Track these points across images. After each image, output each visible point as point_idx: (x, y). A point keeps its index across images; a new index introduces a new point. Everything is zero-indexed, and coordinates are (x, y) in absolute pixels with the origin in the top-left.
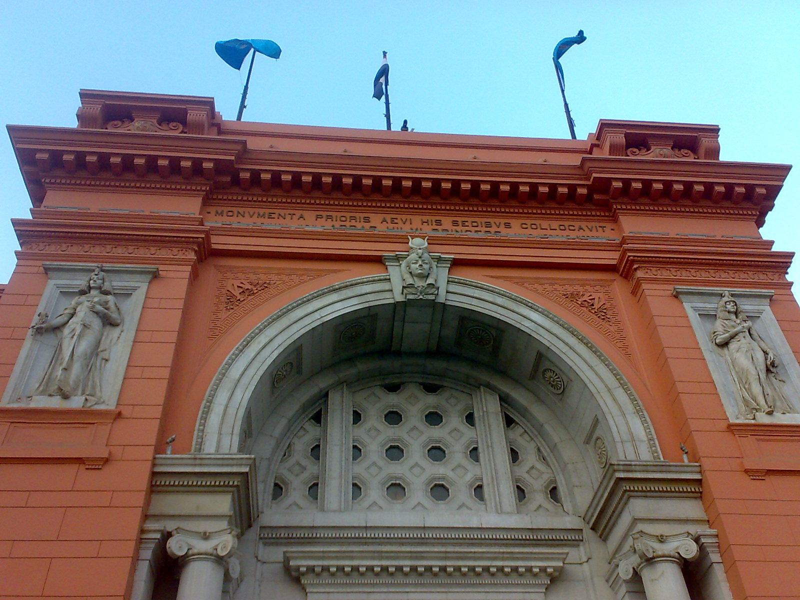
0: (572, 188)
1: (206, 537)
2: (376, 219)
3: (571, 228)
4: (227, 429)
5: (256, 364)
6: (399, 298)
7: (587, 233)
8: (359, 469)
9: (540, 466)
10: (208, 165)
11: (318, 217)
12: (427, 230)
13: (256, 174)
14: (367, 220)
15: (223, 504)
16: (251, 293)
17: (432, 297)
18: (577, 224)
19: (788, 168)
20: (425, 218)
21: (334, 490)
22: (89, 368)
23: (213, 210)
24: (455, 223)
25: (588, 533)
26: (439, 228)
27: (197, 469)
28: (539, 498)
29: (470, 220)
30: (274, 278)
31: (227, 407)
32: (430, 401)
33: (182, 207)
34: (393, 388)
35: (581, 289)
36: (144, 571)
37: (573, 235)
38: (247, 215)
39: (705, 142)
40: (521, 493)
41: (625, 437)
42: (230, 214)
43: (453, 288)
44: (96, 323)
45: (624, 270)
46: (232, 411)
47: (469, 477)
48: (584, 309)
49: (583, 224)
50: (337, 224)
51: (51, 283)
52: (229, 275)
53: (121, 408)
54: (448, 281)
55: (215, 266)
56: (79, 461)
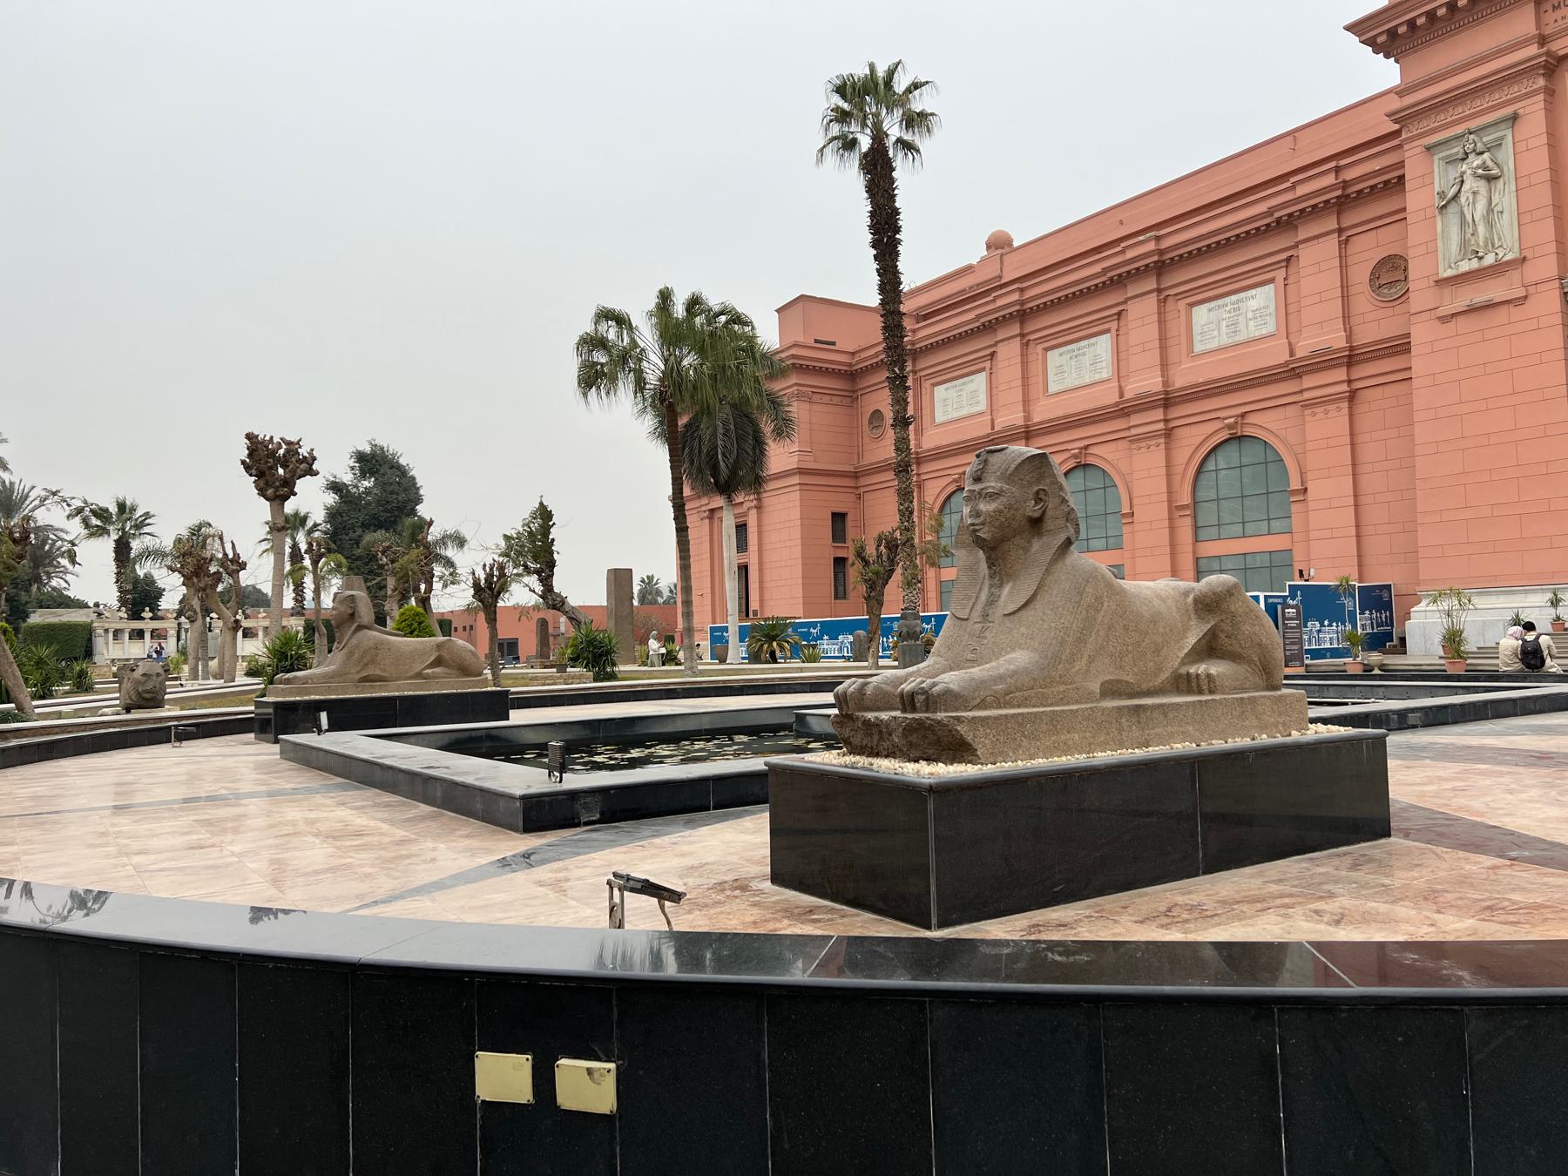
22: (1490, 225)
44: (1482, 186)
51: (1436, 157)
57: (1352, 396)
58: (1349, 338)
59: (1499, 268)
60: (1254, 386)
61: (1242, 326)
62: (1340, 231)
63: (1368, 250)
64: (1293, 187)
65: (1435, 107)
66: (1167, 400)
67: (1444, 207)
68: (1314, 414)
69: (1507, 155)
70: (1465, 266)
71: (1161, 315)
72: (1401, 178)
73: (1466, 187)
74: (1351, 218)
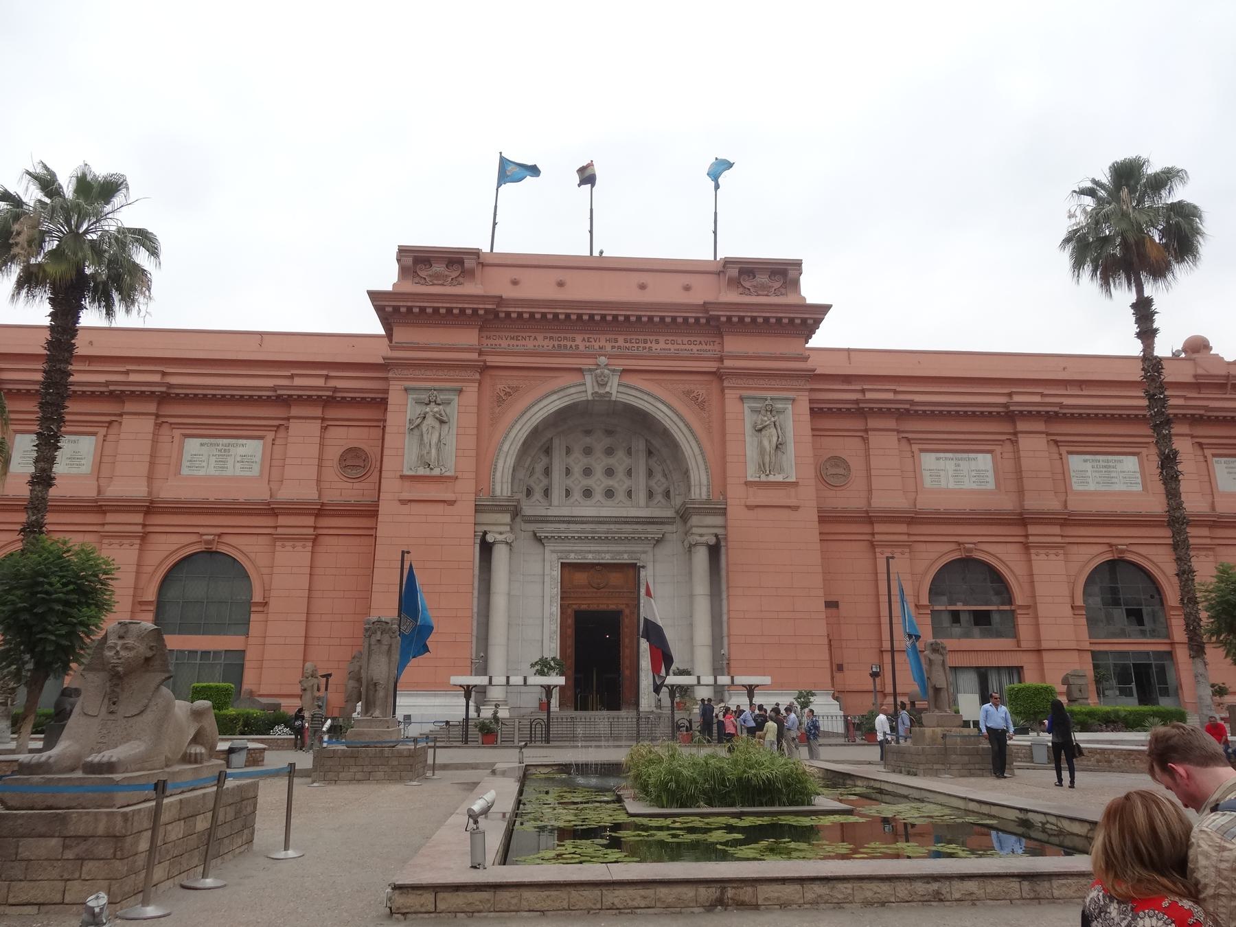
0: (697, 319)
1: (501, 533)
2: (579, 338)
6: (590, 398)
7: (704, 347)
8: (569, 482)
9: (663, 480)
10: (481, 312)
11: (545, 338)
12: (608, 346)
13: (508, 314)
15: (507, 518)
18: (699, 339)
19: (828, 307)
20: (608, 337)
21: (557, 494)
22: (438, 449)
23: (484, 334)
24: (626, 341)
25: (678, 519)
28: (659, 498)
32: (607, 441)
33: (468, 337)
34: (588, 432)
37: (695, 348)
39: (791, 274)
40: (651, 494)
43: (622, 389)
44: (437, 425)
45: (718, 375)
47: (625, 487)
49: (702, 339)
50: (556, 343)
56: (444, 501)
57: (315, 540)
59: (441, 479)
60: (129, 512)
61: (230, 465)
62: (323, 419)
63: (343, 437)
64: (292, 377)
65: (415, 365)
66: (150, 508)
68: (283, 546)
69: (452, 411)
70: (422, 471)
71: (155, 435)
73: (425, 422)
74: (331, 413)
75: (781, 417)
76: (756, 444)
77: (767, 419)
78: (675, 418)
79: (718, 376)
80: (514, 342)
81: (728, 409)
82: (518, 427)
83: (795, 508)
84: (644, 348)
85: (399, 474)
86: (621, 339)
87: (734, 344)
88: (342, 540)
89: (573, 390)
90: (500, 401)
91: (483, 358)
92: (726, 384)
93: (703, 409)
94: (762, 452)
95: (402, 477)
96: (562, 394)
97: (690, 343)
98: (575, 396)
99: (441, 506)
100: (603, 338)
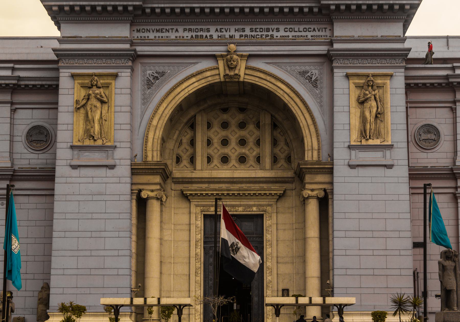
1: (152, 191)
2: (213, 29)
3: (310, 30)
4: (155, 149)
5: (163, 118)
6: (222, 79)
7: (317, 33)
11: (185, 30)
12: (237, 35)
14: (208, 30)
16: (157, 78)
17: (237, 80)
18: (312, 27)
20: (237, 27)
23: (135, 28)
24: (251, 30)
26: (244, 34)
27: (147, 167)
29: (259, 27)
30: (167, 68)
31: (153, 138)
35: (307, 68)
36: (134, 202)
37: (309, 34)
38: (151, 30)
41: (310, 148)
42: (143, 31)
43: (248, 72)
44: (99, 104)
46: (155, 140)
48: (307, 81)
49: (316, 27)
50: (194, 34)
51: (76, 82)
52: (147, 68)
53: (116, 144)
54: (246, 68)
55: (141, 63)
58: (13, 164)
59: (102, 148)
67: (79, 108)
70: (87, 142)
72: (57, 86)
75: (381, 91)
76: (358, 114)
77: (369, 93)
78: (292, 95)
79: (328, 58)
80: (160, 34)
81: (336, 85)
82: (164, 105)
83: (390, 167)
84: (267, 36)
85: (69, 145)
86: (247, 29)
87: (342, 30)
88: (32, 199)
89: (208, 74)
90: (149, 84)
91: (134, 48)
92: (334, 65)
93: (316, 87)
94: (364, 120)
95: (72, 147)
96: (199, 77)
97: (305, 30)
98: (210, 79)
99: (103, 170)
100: (233, 28)
